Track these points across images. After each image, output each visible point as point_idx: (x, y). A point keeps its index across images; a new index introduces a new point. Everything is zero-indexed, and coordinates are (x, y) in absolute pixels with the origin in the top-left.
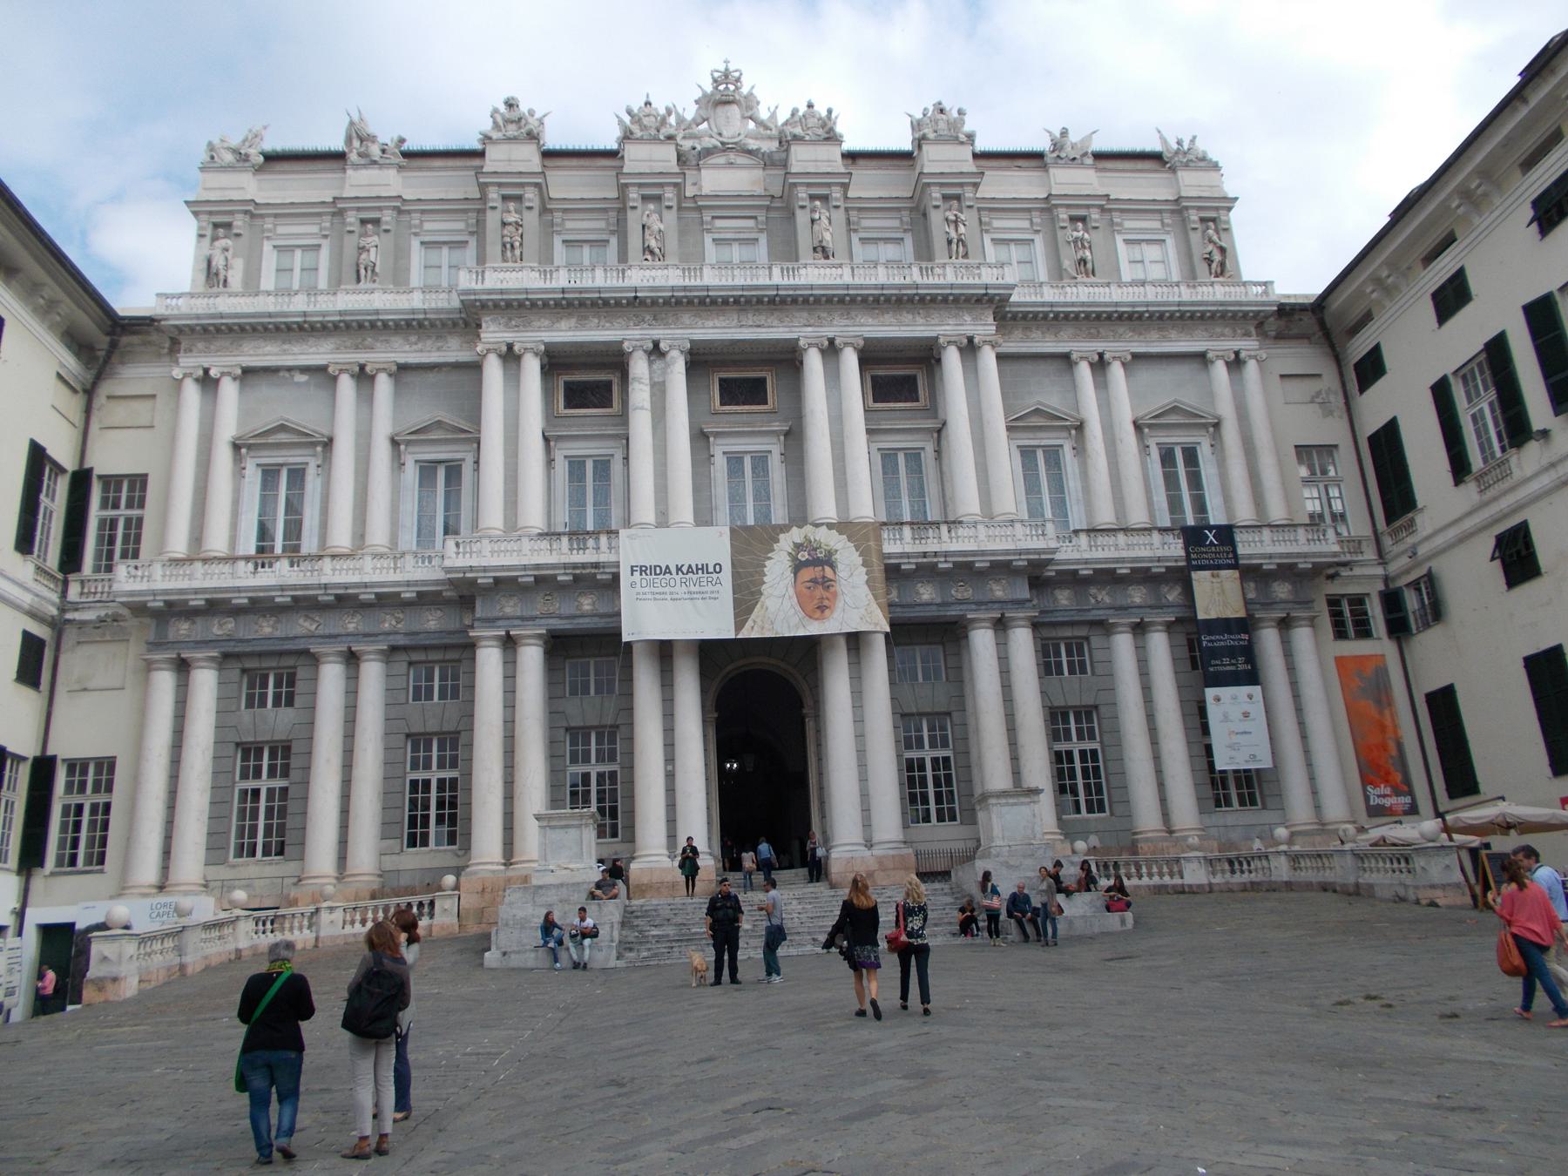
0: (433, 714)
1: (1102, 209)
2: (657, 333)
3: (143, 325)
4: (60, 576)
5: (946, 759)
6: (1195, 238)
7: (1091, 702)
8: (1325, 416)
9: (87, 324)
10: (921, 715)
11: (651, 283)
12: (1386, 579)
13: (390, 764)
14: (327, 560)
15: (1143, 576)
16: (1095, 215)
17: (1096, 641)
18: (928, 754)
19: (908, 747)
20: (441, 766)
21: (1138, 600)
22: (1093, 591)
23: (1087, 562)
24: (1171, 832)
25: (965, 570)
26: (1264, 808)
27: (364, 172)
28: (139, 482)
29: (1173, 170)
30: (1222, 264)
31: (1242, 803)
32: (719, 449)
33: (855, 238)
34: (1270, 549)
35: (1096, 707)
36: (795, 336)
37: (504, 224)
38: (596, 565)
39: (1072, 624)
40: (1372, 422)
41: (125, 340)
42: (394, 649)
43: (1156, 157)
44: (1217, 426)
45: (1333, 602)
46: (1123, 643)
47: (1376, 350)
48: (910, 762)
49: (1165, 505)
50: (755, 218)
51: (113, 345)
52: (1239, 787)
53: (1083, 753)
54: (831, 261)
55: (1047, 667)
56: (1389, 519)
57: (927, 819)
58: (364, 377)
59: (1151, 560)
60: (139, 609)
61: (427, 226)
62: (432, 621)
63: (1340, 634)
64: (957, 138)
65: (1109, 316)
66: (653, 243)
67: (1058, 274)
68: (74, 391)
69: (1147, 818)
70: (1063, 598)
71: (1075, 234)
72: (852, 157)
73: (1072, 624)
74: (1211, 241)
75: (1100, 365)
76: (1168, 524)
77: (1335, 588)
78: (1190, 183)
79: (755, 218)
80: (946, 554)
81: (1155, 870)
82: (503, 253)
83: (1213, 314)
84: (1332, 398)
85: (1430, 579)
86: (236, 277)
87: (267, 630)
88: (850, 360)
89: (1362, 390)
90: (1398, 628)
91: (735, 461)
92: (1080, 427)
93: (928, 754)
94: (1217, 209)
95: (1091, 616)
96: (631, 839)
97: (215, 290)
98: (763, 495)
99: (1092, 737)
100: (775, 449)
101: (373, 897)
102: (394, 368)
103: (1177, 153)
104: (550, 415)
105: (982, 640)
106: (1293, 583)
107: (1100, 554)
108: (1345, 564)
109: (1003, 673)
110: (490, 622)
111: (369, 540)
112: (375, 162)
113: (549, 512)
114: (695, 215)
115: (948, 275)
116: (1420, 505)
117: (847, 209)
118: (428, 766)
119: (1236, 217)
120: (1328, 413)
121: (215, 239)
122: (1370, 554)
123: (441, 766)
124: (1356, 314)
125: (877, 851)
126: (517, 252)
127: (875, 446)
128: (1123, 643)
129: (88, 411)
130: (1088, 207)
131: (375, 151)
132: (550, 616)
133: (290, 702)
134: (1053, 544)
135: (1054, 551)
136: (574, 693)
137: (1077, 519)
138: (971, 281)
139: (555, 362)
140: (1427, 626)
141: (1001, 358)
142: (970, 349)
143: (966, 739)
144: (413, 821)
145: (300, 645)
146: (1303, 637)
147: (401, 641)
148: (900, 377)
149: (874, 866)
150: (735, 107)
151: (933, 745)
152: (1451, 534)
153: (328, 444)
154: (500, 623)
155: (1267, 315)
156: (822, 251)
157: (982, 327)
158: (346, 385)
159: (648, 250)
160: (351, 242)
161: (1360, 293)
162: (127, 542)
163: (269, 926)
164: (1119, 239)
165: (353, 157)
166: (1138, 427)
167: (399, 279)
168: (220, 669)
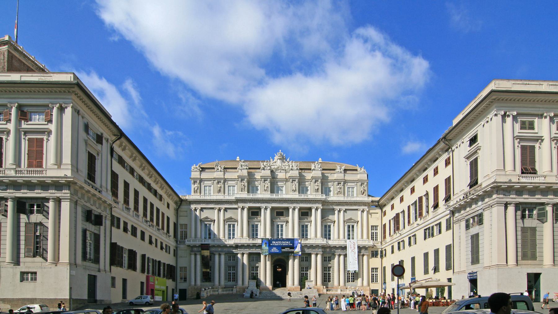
0: (231, 263)
3: (186, 200)
9: (178, 199)
13: (225, 270)
16: (342, 183)
25: (312, 247)
43: (356, 170)
60: (189, 246)
69: (336, 283)
70: (328, 250)
88: (297, 210)
90: (382, 257)
92: (335, 222)
97: (196, 194)
100: (285, 224)
105: (313, 257)
122: (380, 244)
129: (177, 213)
131: (219, 168)
141: (322, 210)
148: (305, 213)
157: (320, 206)
158: (216, 211)
162: (185, 236)
166: (344, 222)
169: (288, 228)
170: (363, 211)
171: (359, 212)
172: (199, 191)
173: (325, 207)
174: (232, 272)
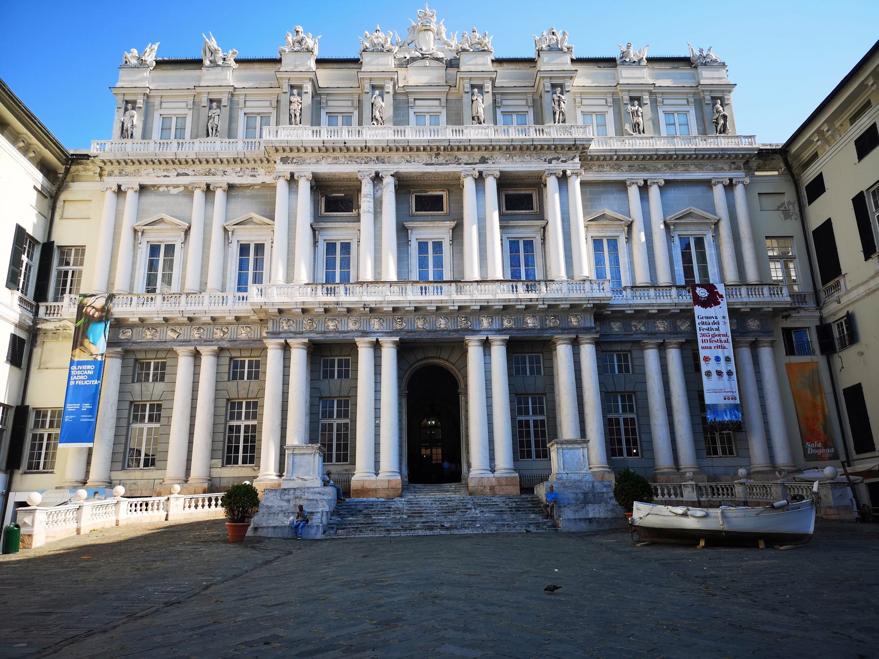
1: (651, 93)
2: (379, 167)
4: (34, 303)
5: (543, 421)
6: (708, 109)
7: (629, 388)
8: (786, 219)
10: (530, 394)
11: (375, 138)
12: (821, 319)
14: (183, 297)
15: (663, 314)
17: (635, 353)
18: (531, 418)
19: (520, 413)
20: (247, 418)
21: (662, 329)
22: (634, 323)
23: (630, 305)
24: (678, 469)
26: (738, 456)
27: (212, 70)
28: (81, 250)
29: (696, 67)
30: (725, 125)
31: (724, 452)
32: (415, 237)
33: (498, 111)
34: (745, 299)
35: (634, 392)
36: (460, 170)
37: (291, 102)
38: (337, 303)
39: (621, 342)
40: (815, 222)
41: (73, 168)
42: (221, 349)
44: (717, 224)
45: (787, 332)
46: (651, 356)
47: (820, 178)
48: (520, 422)
49: (682, 273)
50: (440, 99)
51: (67, 171)
52: (722, 443)
53: (625, 420)
54: (483, 125)
55: (603, 369)
56: (824, 284)
57: (529, 456)
58: (209, 191)
59: (670, 305)
61: (248, 104)
62: (243, 333)
63: (790, 351)
64: (561, 50)
65: (651, 157)
66: (377, 115)
67: (620, 132)
68: (46, 197)
69: (663, 459)
70: (616, 327)
71: (633, 108)
72: (498, 61)
73: (621, 342)
74: (718, 112)
75: (644, 189)
76: (683, 283)
77: (788, 324)
78: (707, 77)
79: (440, 99)
80: (544, 300)
81: (666, 491)
82: (290, 119)
83: (716, 156)
84: (791, 207)
85: (850, 319)
86: (138, 132)
87: (149, 337)
88: (491, 185)
89: (810, 203)
91: (423, 246)
92: (630, 226)
93: (531, 418)
94: (723, 91)
95: (632, 338)
96: (354, 463)
98: (439, 263)
99: (631, 411)
101: (204, 492)
102: (226, 186)
103: (699, 58)
104: (317, 217)
105: (563, 352)
106: (761, 321)
107: (638, 301)
108: (794, 309)
109: (575, 372)
110: (275, 334)
111: (209, 286)
112: (219, 66)
113: (314, 273)
114: (404, 97)
115: (553, 133)
116: (843, 273)
117: (494, 94)
118: (239, 418)
119: (733, 98)
120: (787, 215)
121: (126, 110)
122: (811, 304)
123: (247, 418)
124: (806, 155)
125: (497, 474)
126: (298, 119)
127: (505, 236)
128: (651, 356)
129: (53, 209)
130: (642, 91)
132: (311, 332)
133: (162, 379)
134: (609, 295)
135: (610, 299)
136: (325, 377)
137: (625, 281)
138: (566, 136)
139: (319, 185)
140: (844, 346)
141: (582, 183)
142: (563, 179)
143: (554, 409)
144: (229, 448)
145: (168, 346)
146: (766, 354)
147: (226, 345)
149: (494, 483)
150: (431, 33)
151: (534, 413)
152: (861, 290)
153: (187, 232)
154: (282, 336)
155: (751, 156)
156: (476, 119)
157: (573, 165)
158: (198, 195)
159: (373, 118)
160: (205, 112)
161: (809, 142)
163: (139, 507)
164: (660, 111)
165: (207, 63)
166: (666, 225)
167: (231, 134)
168: (123, 358)
169: (461, 252)
170: (729, 187)
171: (719, 192)
172: (138, 132)
173: (591, 176)
174: (243, 423)
